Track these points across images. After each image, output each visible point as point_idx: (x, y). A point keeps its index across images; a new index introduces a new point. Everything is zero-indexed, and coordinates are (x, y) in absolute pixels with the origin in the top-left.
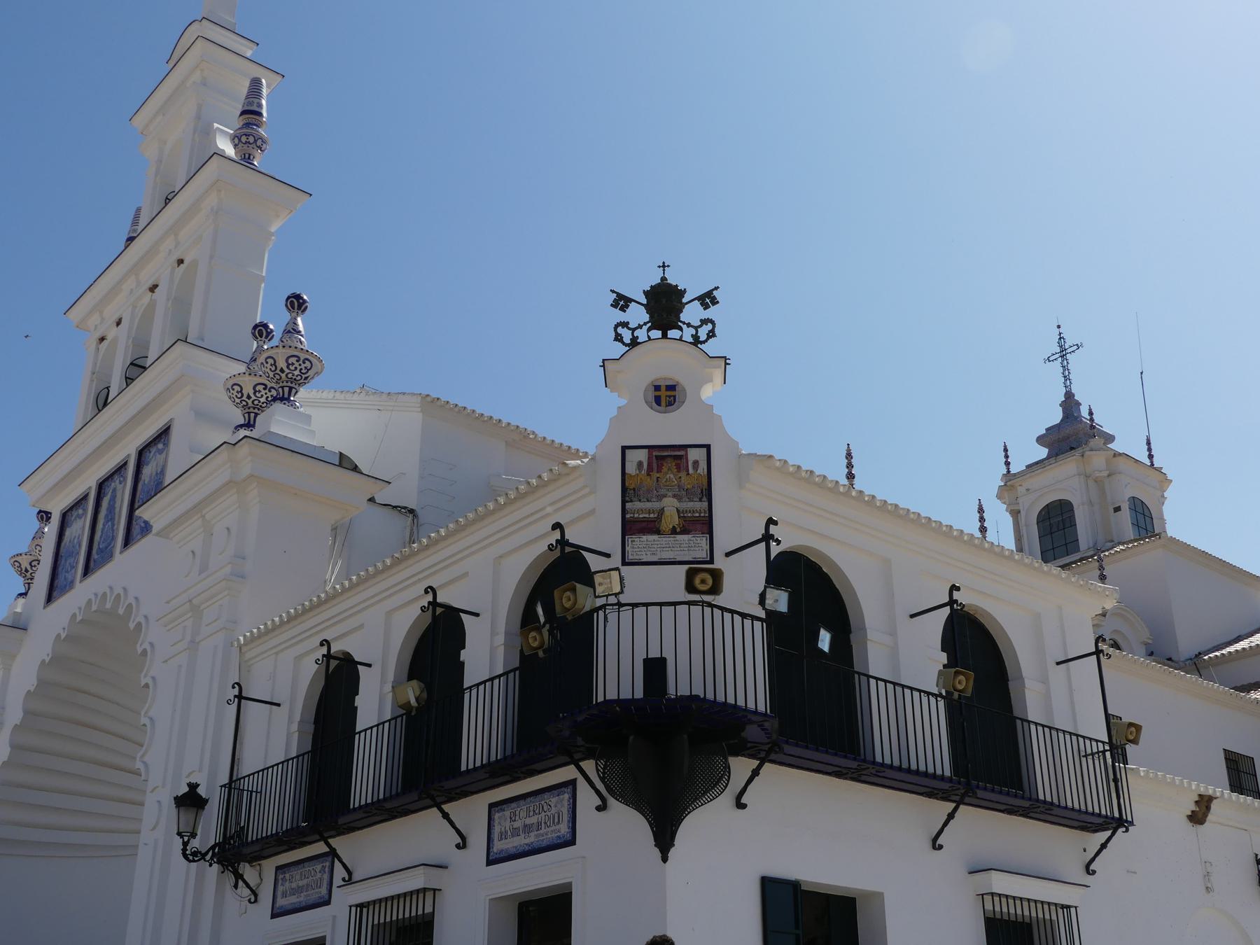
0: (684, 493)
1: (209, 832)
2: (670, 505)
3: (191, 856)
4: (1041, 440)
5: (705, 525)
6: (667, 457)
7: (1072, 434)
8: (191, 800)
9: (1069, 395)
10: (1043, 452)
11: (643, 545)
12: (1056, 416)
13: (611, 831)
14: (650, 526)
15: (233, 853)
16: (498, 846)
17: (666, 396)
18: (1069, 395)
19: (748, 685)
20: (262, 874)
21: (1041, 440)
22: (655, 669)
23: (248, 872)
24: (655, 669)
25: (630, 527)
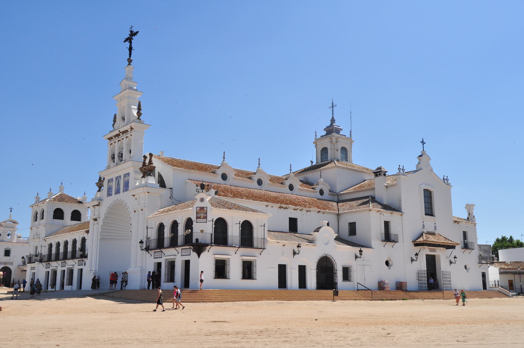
0: (204, 213)
1: (144, 247)
2: (202, 215)
3: (142, 250)
4: (325, 129)
5: (206, 218)
6: (202, 208)
7: (331, 130)
8: (141, 242)
9: (333, 118)
10: (325, 133)
11: (199, 220)
12: (329, 124)
13: (194, 255)
14: (199, 218)
15: (147, 249)
16: (183, 254)
17: (202, 200)
18: (333, 118)
19: (208, 241)
20: (152, 252)
21: (325, 129)
22: (197, 240)
23: (150, 251)
24: (197, 240)
25: (197, 218)
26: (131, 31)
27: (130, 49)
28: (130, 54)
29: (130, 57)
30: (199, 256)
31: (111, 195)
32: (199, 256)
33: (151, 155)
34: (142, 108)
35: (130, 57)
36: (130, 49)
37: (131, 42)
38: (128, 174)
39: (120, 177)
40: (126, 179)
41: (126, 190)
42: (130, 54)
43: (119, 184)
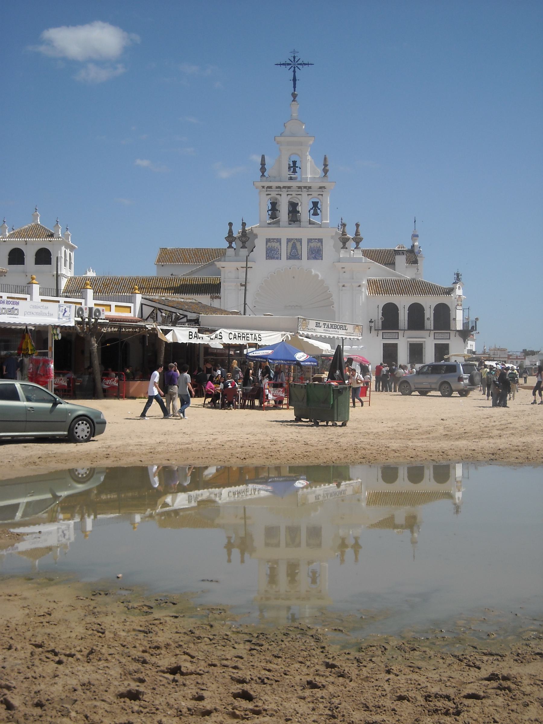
8: (371, 322)
26: (294, 57)
27: (294, 80)
28: (295, 87)
29: (295, 91)
30: (464, 341)
31: (277, 258)
32: (464, 341)
33: (357, 225)
34: (329, 162)
35: (295, 91)
36: (294, 80)
37: (294, 71)
38: (320, 241)
39: (300, 241)
40: (312, 245)
41: (315, 258)
42: (295, 87)
43: (294, 247)
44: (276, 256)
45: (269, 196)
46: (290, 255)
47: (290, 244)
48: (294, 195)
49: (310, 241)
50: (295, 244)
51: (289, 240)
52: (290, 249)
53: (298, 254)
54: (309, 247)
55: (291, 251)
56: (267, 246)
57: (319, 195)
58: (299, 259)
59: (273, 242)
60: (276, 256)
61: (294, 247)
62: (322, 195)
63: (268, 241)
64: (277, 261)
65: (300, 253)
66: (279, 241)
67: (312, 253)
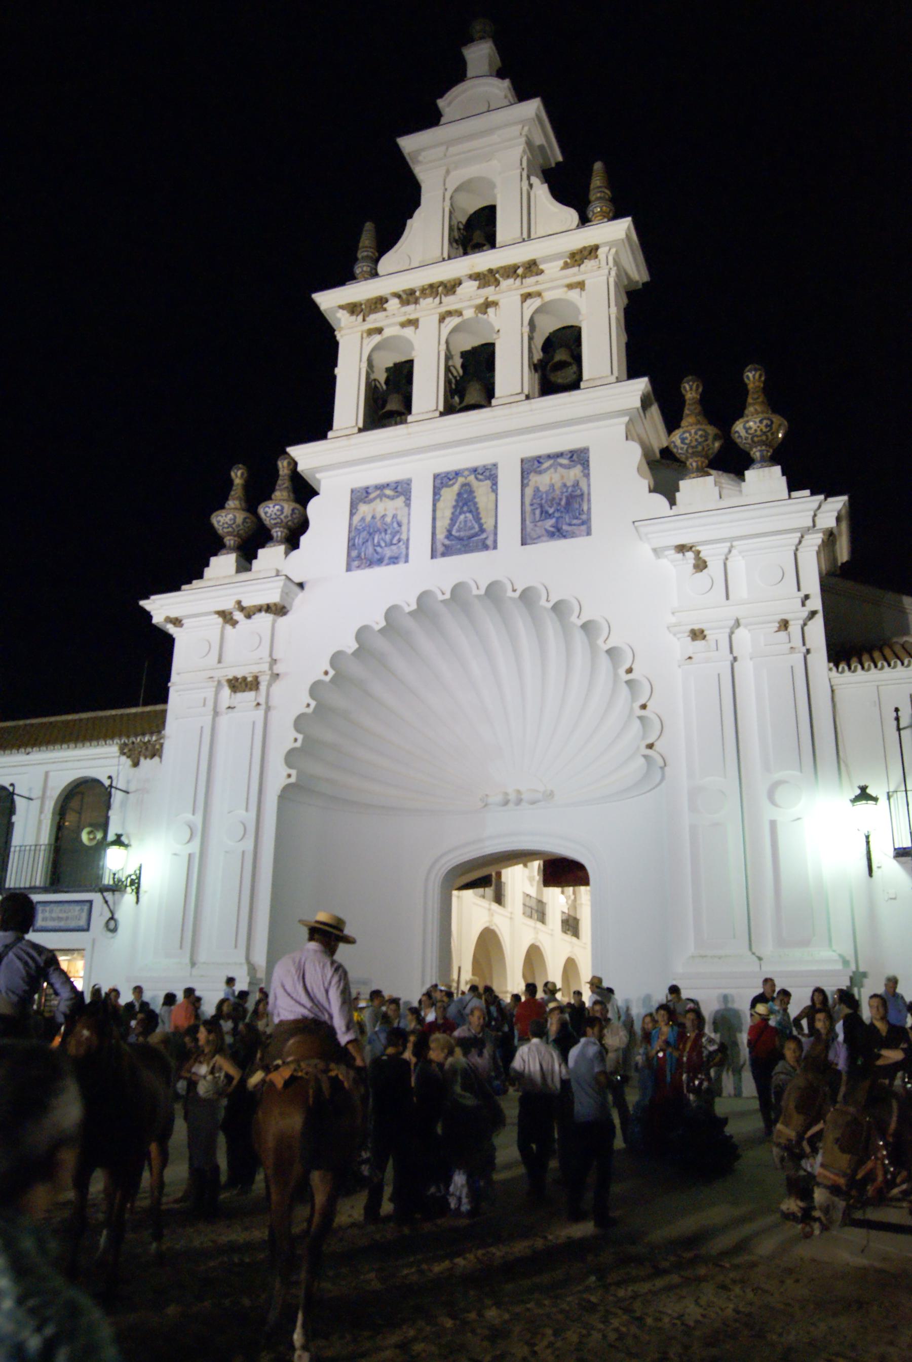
31: (394, 560)
38: (579, 458)
40: (543, 481)
41: (558, 533)
44: (388, 552)
45: (377, 338)
46: (449, 535)
47: (449, 495)
48: (469, 313)
49: (531, 466)
50: (471, 492)
51: (441, 481)
52: (448, 513)
53: (482, 530)
54: (529, 491)
55: (453, 520)
56: (356, 519)
57: (570, 286)
58: (486, 547)
59: (381, 497)
60: (388, 552)
61: (466, 501)
62: (581, 285)
63: (360, 497)
64: (392, 568)
65: (488, 524)
66: (401, 489)
67: (545, 515)
